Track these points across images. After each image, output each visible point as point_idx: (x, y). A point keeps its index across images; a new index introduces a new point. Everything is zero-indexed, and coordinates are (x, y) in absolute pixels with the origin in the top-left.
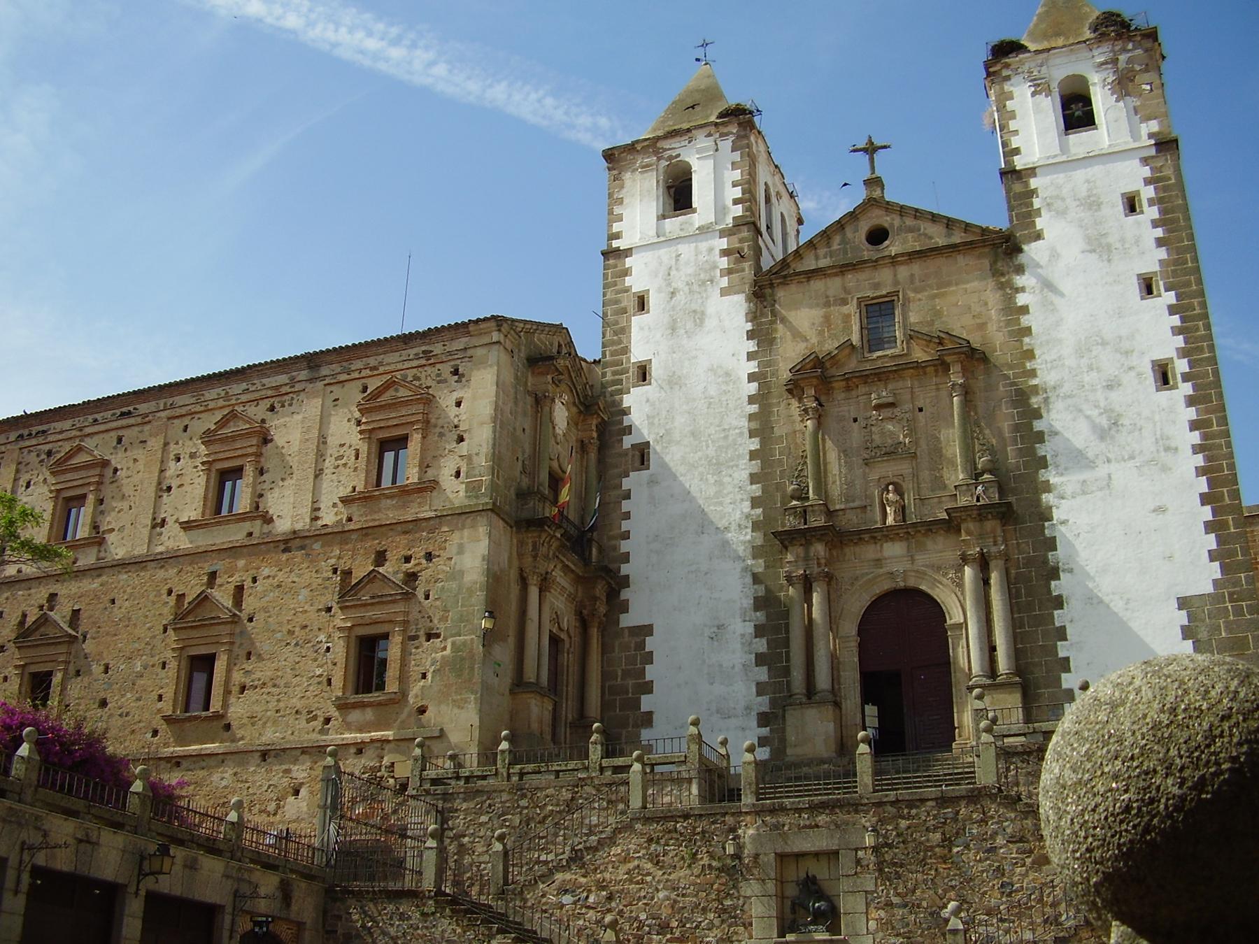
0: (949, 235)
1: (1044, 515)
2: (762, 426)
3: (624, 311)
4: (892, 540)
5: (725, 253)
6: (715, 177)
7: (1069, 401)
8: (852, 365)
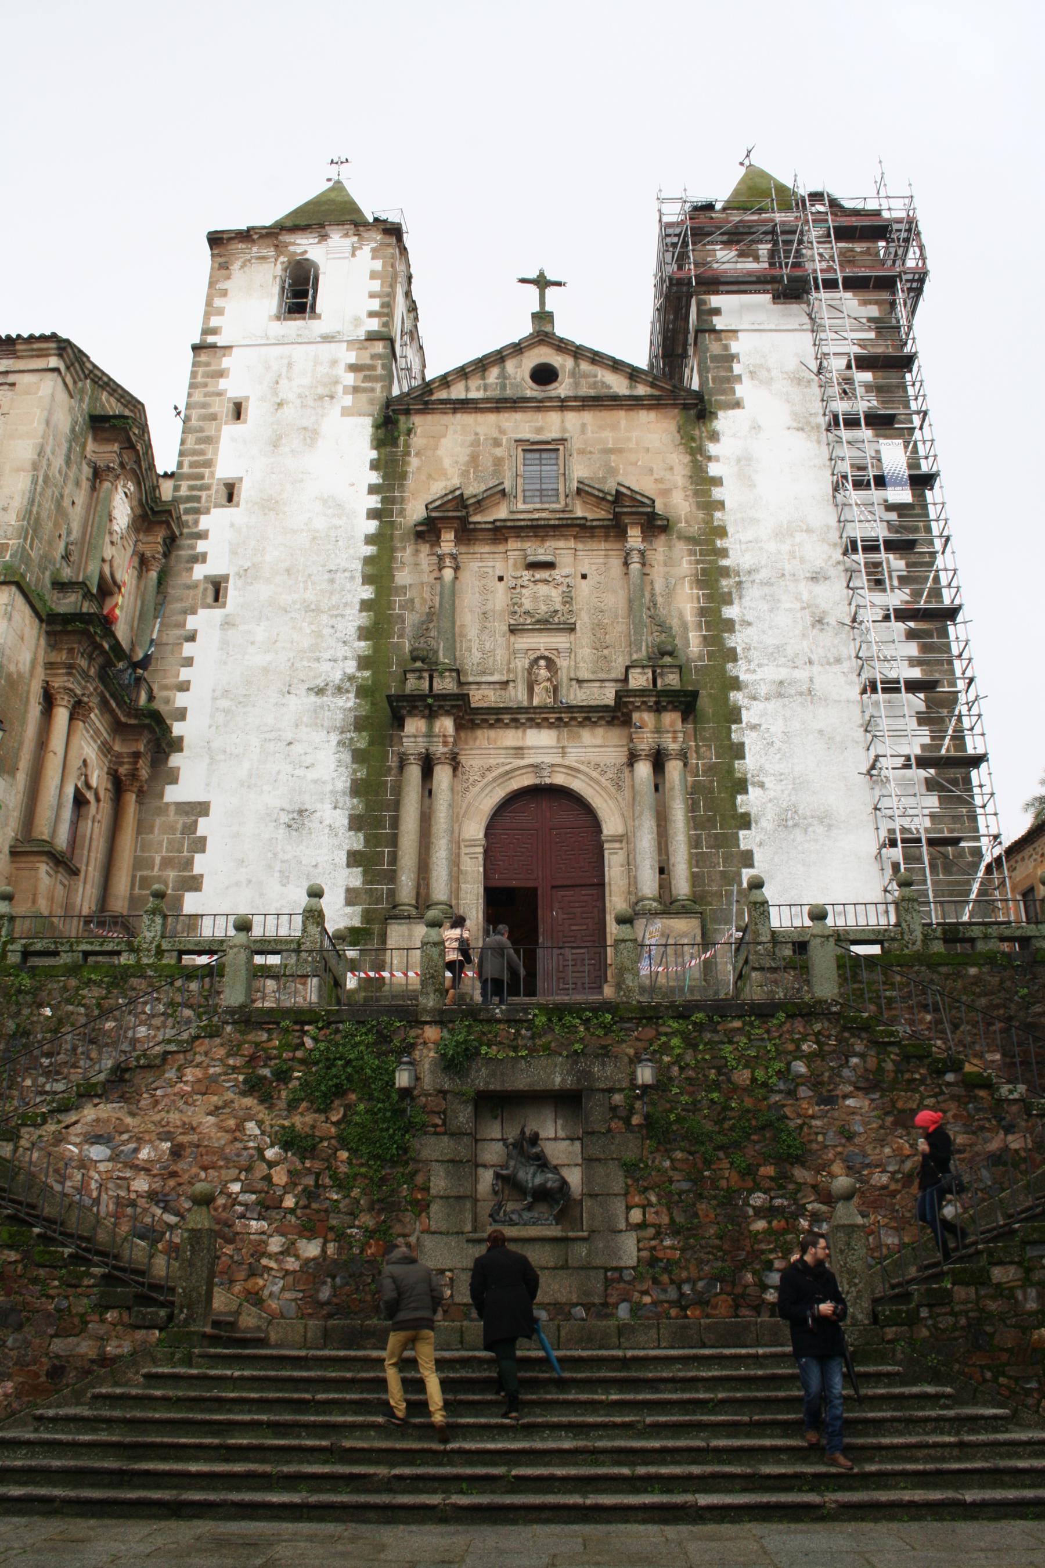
0: (631, 387)
1: (734, 715)
2: (379, 571)
3: (214, 417)
4: (538, 726)
5: (353, 368)
6: (347, 275)
7: (767, 590)
8: (501, 513)
